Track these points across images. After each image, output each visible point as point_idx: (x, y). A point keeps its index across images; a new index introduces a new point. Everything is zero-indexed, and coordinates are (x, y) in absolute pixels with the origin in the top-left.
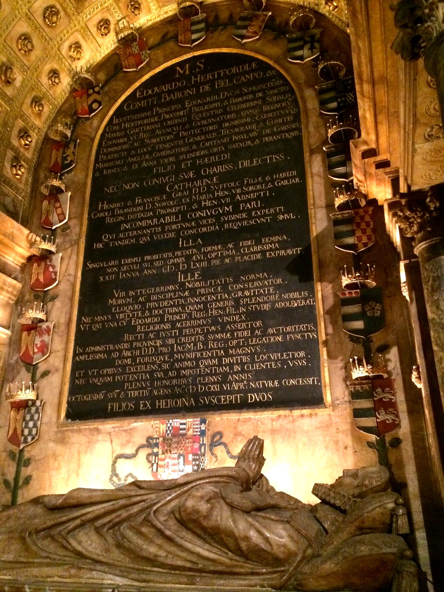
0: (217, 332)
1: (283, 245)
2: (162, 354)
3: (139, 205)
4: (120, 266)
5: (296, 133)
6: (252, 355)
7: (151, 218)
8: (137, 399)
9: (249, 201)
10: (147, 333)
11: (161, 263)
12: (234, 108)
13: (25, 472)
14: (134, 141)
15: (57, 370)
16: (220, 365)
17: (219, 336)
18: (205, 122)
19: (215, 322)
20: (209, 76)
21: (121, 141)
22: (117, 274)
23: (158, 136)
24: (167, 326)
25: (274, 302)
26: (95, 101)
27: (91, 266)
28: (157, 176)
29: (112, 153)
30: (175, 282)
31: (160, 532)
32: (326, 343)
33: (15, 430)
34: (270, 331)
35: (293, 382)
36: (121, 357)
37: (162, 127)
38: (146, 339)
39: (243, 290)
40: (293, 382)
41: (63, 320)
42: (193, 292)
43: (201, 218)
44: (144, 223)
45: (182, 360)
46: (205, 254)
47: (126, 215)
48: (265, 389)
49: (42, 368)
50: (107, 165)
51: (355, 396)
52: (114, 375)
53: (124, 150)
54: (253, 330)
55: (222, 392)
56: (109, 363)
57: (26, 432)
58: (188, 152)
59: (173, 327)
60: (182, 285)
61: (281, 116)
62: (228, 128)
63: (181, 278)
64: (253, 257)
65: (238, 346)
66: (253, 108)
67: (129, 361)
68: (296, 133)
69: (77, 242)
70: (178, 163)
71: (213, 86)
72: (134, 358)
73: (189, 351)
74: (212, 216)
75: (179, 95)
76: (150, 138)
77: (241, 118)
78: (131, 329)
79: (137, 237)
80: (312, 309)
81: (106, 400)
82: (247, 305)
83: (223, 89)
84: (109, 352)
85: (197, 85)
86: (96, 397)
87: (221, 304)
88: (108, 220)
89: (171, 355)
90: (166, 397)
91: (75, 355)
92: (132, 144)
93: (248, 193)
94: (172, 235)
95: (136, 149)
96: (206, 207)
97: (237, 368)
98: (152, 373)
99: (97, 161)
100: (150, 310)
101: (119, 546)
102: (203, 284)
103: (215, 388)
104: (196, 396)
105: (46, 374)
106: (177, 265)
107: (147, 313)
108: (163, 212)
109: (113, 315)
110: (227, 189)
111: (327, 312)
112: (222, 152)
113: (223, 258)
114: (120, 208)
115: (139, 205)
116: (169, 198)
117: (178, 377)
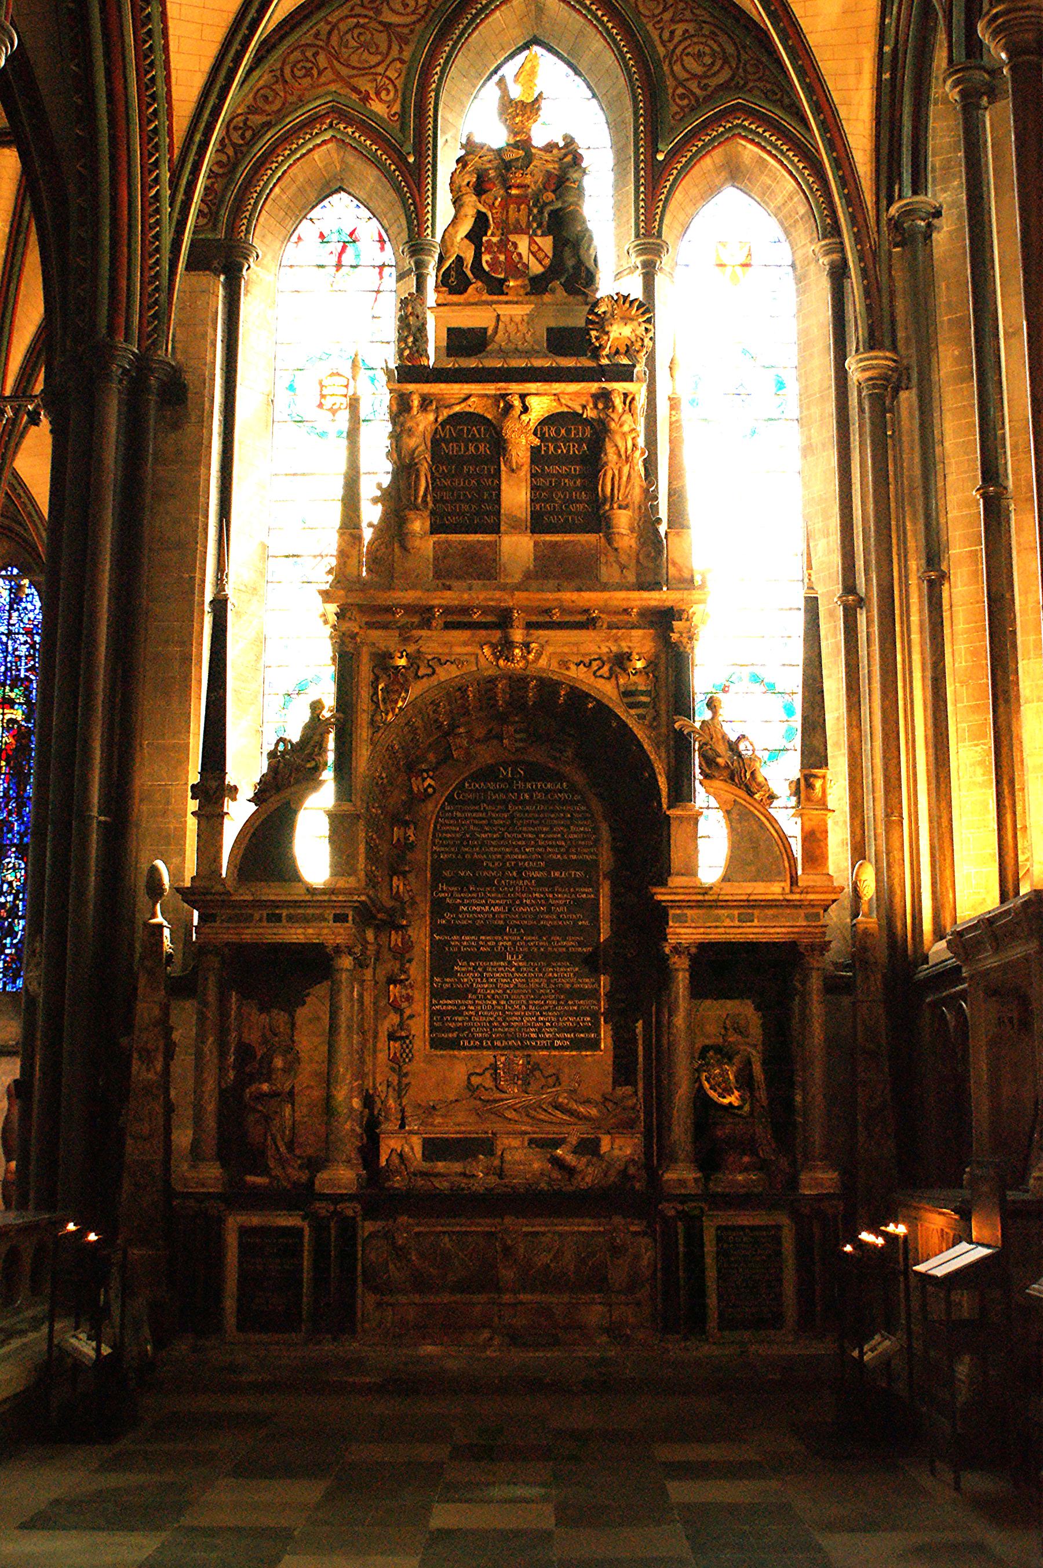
0: (534, 999)
1: (580, 944)
2: (498, 1010)
3: (473, 892)
4: (461, 941)
5: (594, 857)
6: (558, 1016)
7: (483, 905)
8: (481, 1040)
9: (558, 905)
10: (485, 996)
11: (494, 943)
12: (548, 822)
13: (405, 1080)
14: (466, 832)
15: (419, 1015)
16: (537, 1021)
17: (536, 1002)
18: (525, 829)
19: (534, 992)
20: (529, 786)
21: (454, 829)
22: (460, 948)
23: (486, 832)
24: (500, 991)
25: (573, 984)
26: (430, 786)
27: (437, 938)
28: (487, 868)
29: (445, 838)
30: (504, 960)
31: (546, 1111)
32: (602, 1014)
33: (395, 1054)
34: (570, 1002)
35: (582, 1035)
36: (467, 1010)
37: (489, 825)
38: (486, 999)
39: (553, 973)
40: (582, 1035)
41: (419, 979)
42: (518, 969)
43: (525, 913)
44: (478, 909)
45: (510, 1016)
46: (526, 942)
47: (462, 898)
48: (566, 1039)
49: (408, 1012)
50: (442, 849)
51: (616, 1047)
52: (463, 1021)
53: (458, 839)
54: (559, 1000)
55: (538, 1038)
56: (460, 1013)
57: (404, 1055)
58: (511, 853)
59: (505, 992)
60: (510, 962)
61: (583, 839)
62: (545, 839)
63: (509, 957)
64: (560, 950)
65: (549, 1010)
66: (563, 825)
67: (473, 1013)
68: (594, 857)
69: (424, 916)
70: (503, 861)
71: (531, 797)
72: (477, 1013)
73: (516, 1010)
74: (531, 913)
75: (502, 796)
76: (480, 833)
77: (554, 833)
78: (475, 992)
79: (474, 920)
80: (597, 991)
81: (459, 1038)
82: (555, 984)
83: (539, 802)
84: (458, 1006)
85: (519, 791)
86: (450, 1035)
87: (537, 980)
88: (448, 900)
89: (504, 1012)
90: (499, 1039)
91: (432, 1005)
92: (464, 834)
93: (558, 899)
94: (501, 922)
95: (468, 840)
96: (526, 904)
97: (548, 1024)
98: (490, 1022)
99: (433, 843)
100: (487, 978)
101: (528, 1115)
102: (525, 964)
103: (533, 1035)
104: (522, 1040)
105: (411, 1017)
106: (506, 947)
107: (484, 980)
108: (493, 902)
109: (459, 979)
110: (543, 893)
111: (605, 995)
112: (539, 860)
113: (539, 947)
114: (458, 891)
115: (473, 892)
116: (497, 891)
117: (509, 1026)
